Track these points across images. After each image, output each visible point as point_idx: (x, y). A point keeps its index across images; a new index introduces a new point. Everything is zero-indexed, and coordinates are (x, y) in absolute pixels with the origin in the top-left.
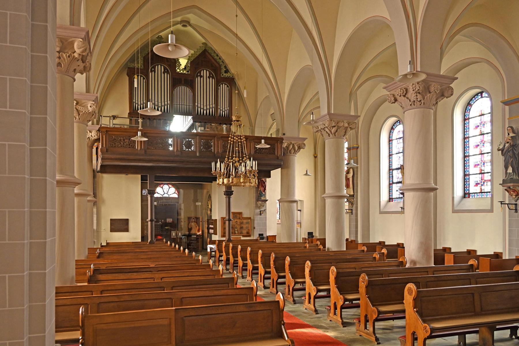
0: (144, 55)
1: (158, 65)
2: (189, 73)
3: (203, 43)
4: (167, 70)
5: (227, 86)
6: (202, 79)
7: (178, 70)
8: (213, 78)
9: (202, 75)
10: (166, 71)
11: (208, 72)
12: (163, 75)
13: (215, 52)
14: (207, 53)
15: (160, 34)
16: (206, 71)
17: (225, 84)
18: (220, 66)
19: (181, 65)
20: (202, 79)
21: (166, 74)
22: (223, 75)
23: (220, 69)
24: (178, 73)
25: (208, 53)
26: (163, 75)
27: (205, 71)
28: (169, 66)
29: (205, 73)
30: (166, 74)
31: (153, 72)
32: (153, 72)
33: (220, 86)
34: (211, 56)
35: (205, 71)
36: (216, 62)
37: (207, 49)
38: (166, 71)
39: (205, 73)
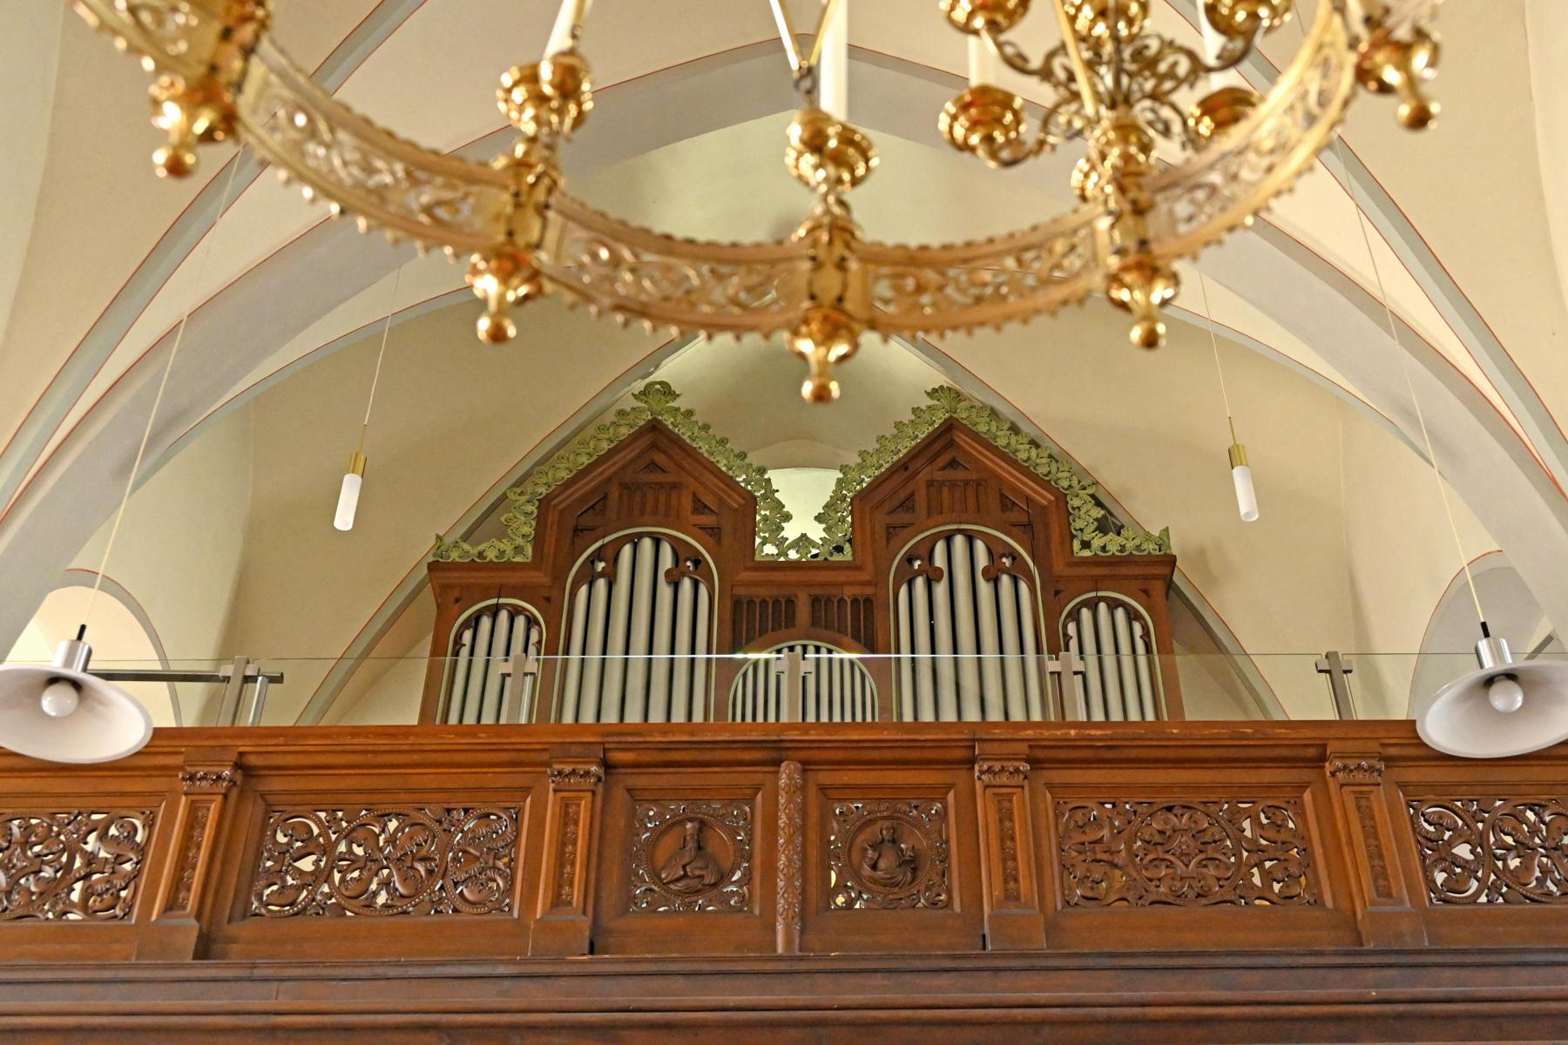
0: (543, 490)
1: (635, 541)
2: (847, 555)
3: (933, 393)
4: (698, 562)
5: (1132, 616)
6: (941, 590)
7: (770, 549)
8: (1018, 573)
9: (940, 560)
10: (687, 564)
11: (980, 546)
12: (665, 592)
13: (1014, 429)
14: (961, 439)
15: (659, 375)
16: (970, 539)
17: (1113, 605)
18: (1061, 498)
19: (788, 517)
20: (941, 590)
21: (686, 584)
22: (1086, 545)
23: (1067, 514)
24: (772, 566)
25: (976, 437)
26: (665, 592)
27: (959, 541)
28: (713, 534)
29: (960, 557)
30: (686, 584)
31: (601, 584)
32: (601, 584)
33: (1075, 616)
34: (995, 450)
35: (959, 541)
36: (1035, 478)
37: (962, 415)
38: (687, 564)
39: (960, 557)
